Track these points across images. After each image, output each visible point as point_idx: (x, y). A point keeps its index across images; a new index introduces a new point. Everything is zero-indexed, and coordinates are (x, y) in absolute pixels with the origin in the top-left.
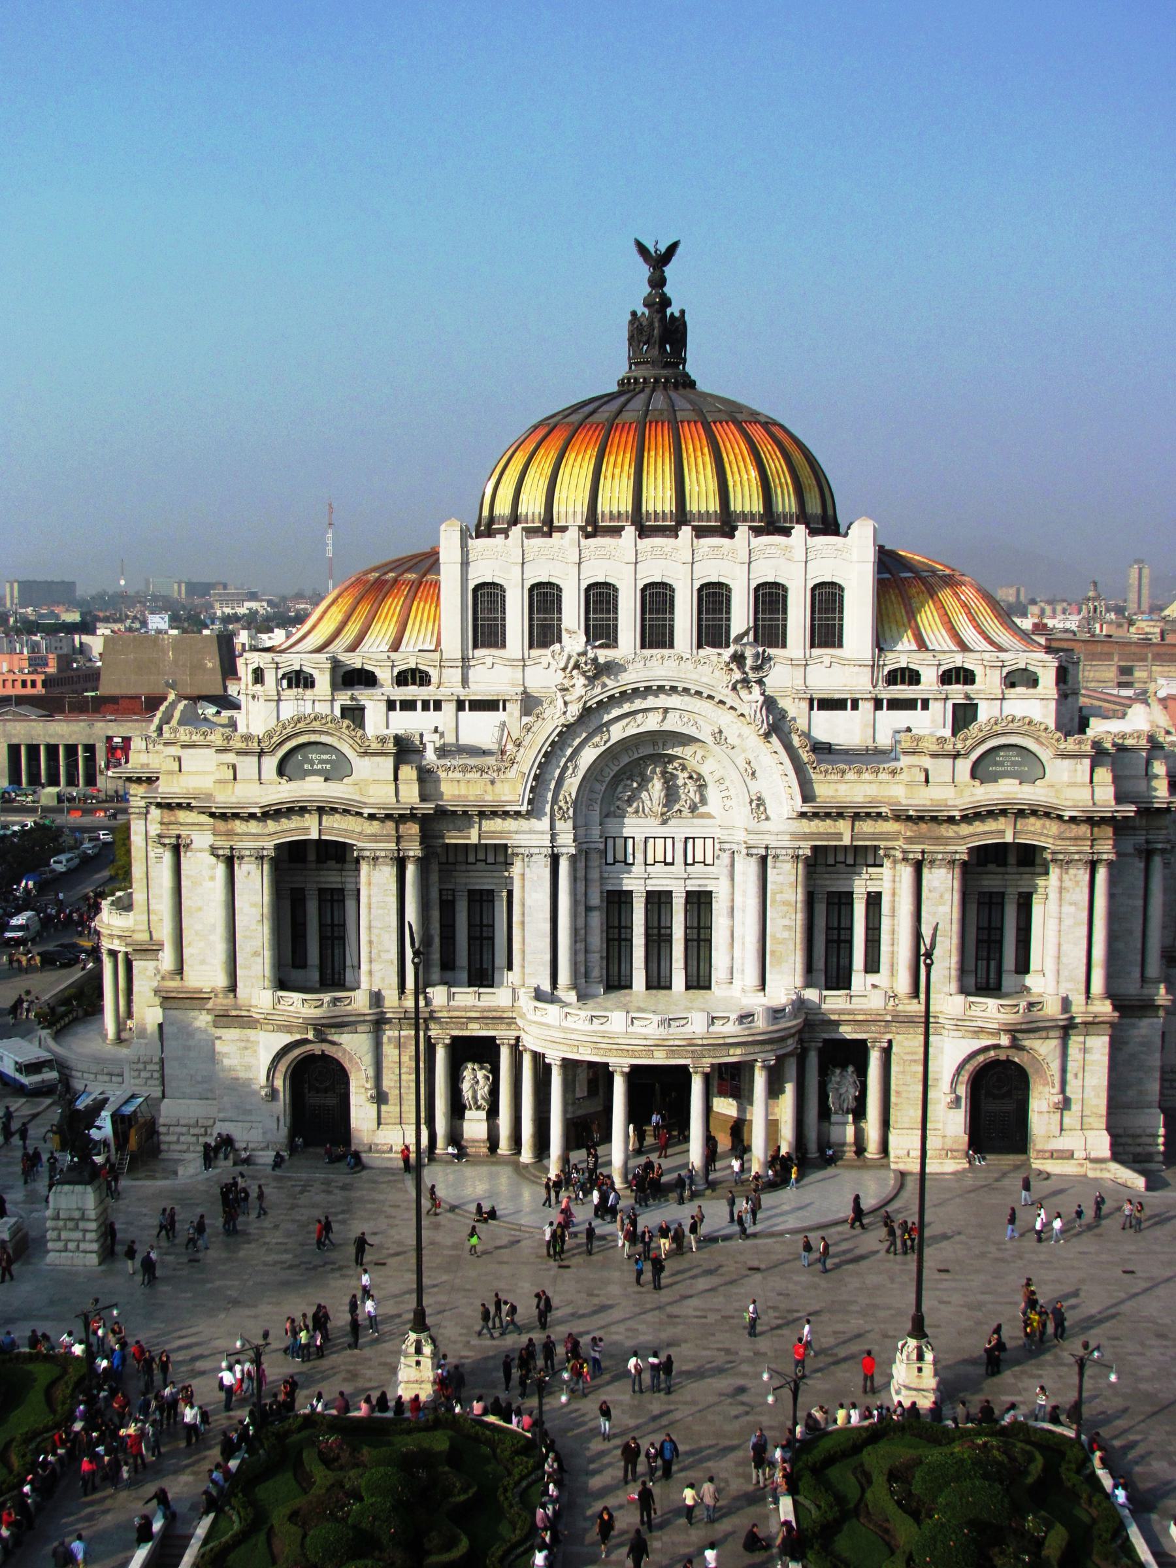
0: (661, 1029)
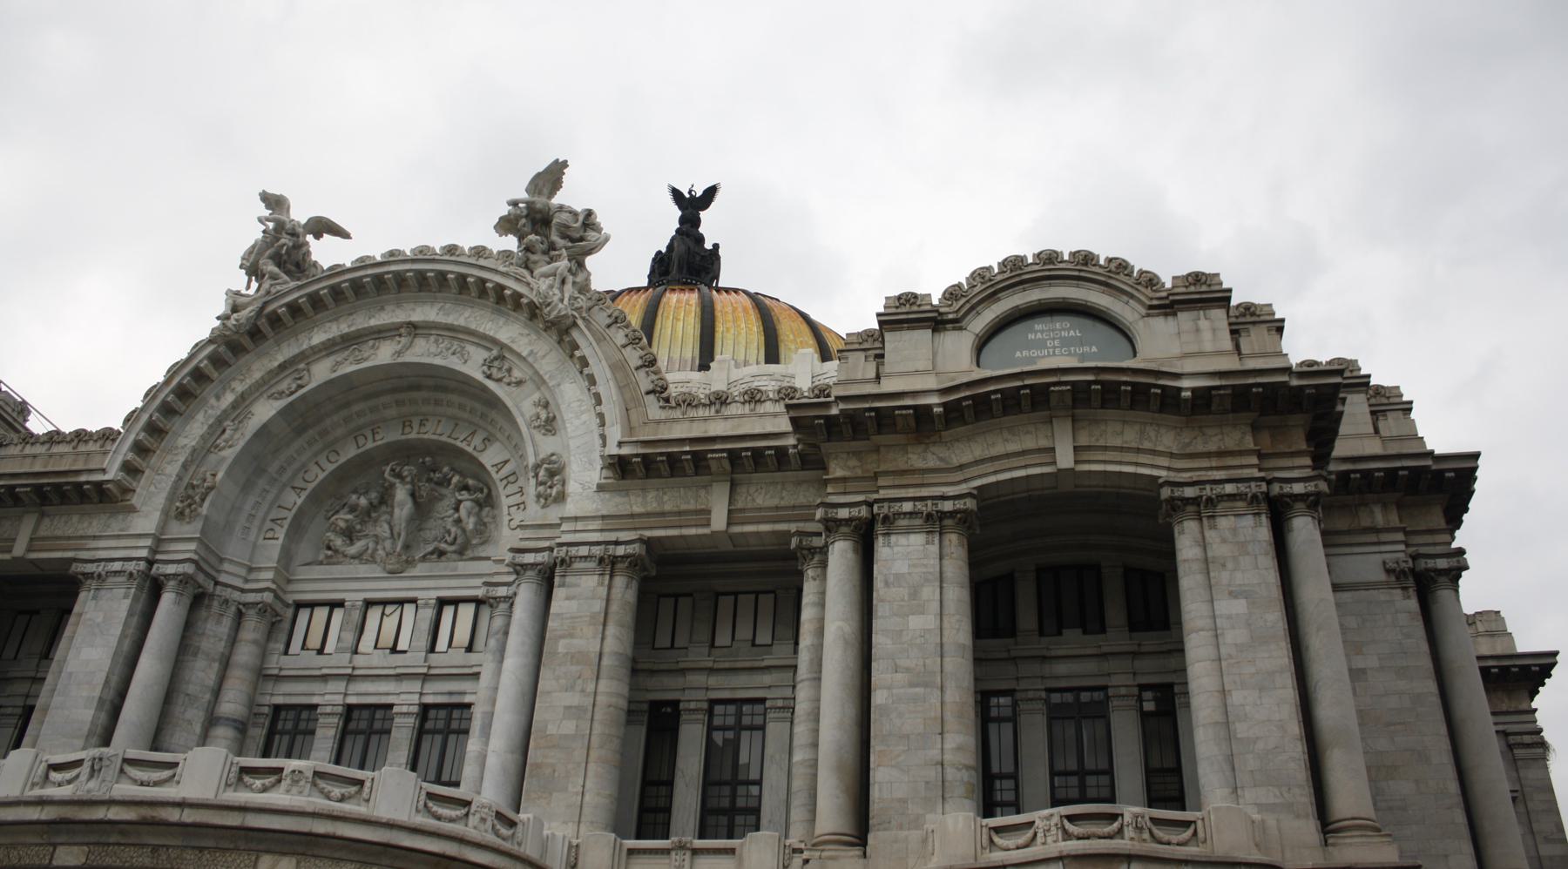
0: (92, 784)
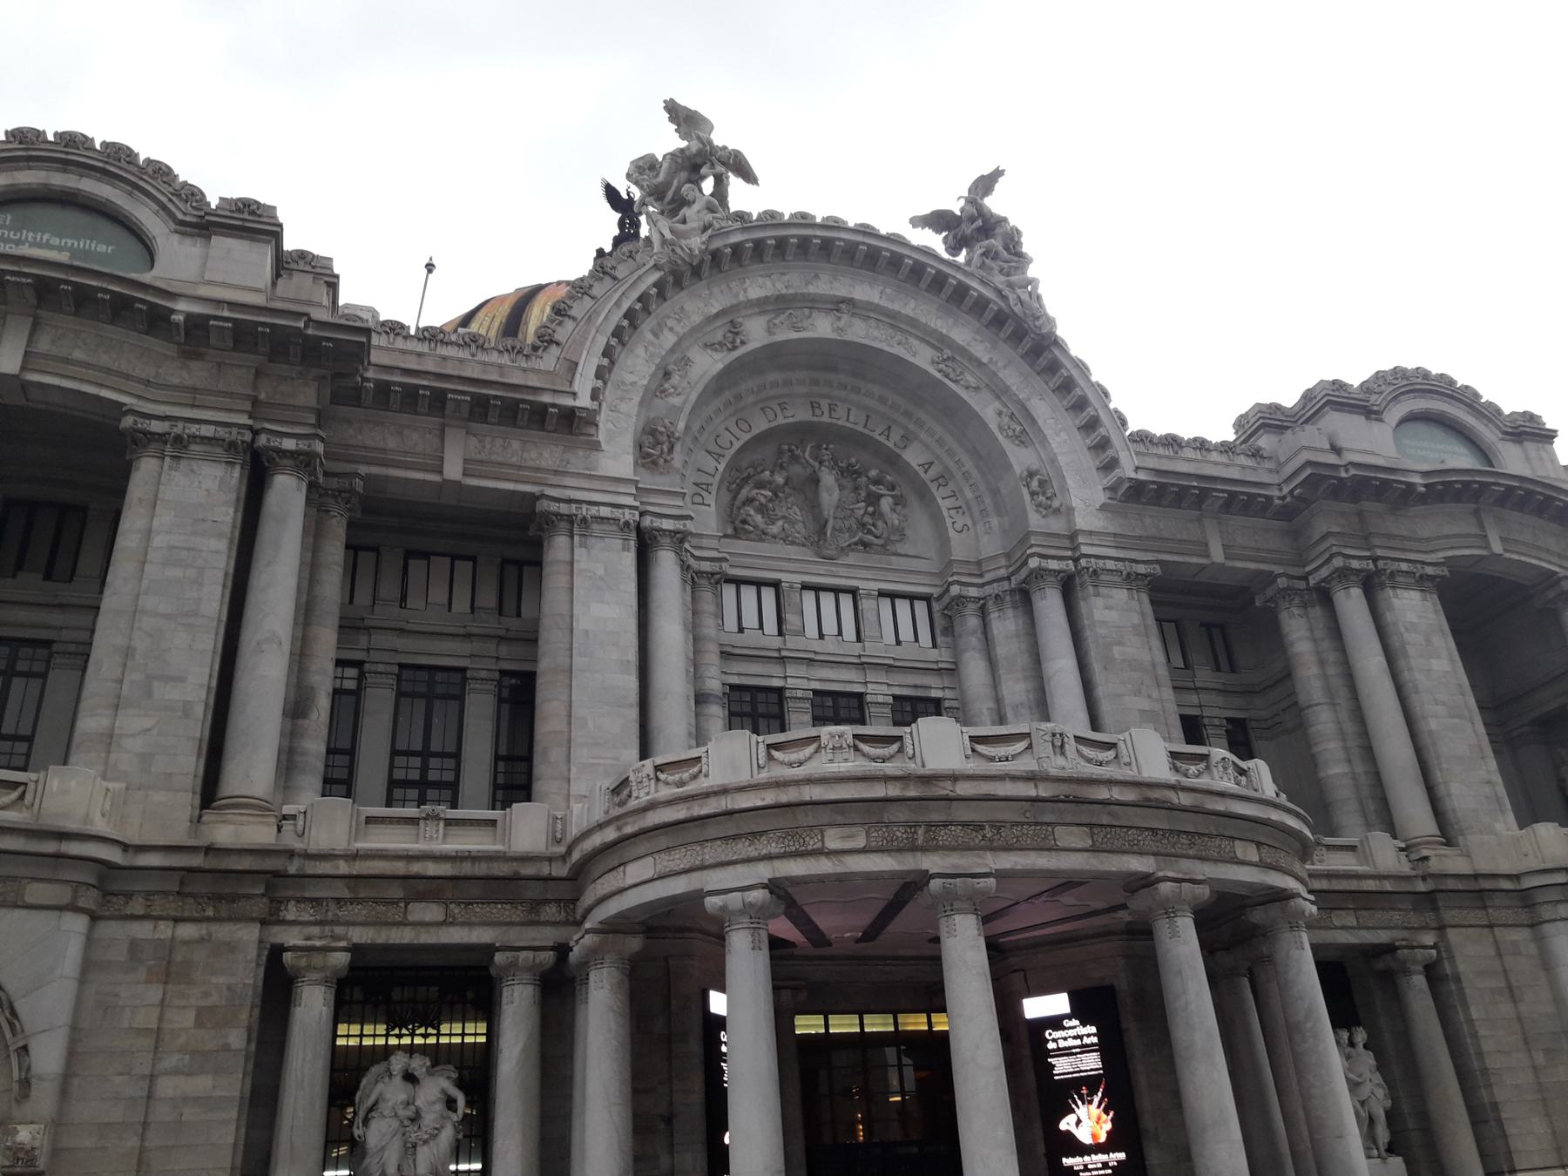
0: (1061, 761)
